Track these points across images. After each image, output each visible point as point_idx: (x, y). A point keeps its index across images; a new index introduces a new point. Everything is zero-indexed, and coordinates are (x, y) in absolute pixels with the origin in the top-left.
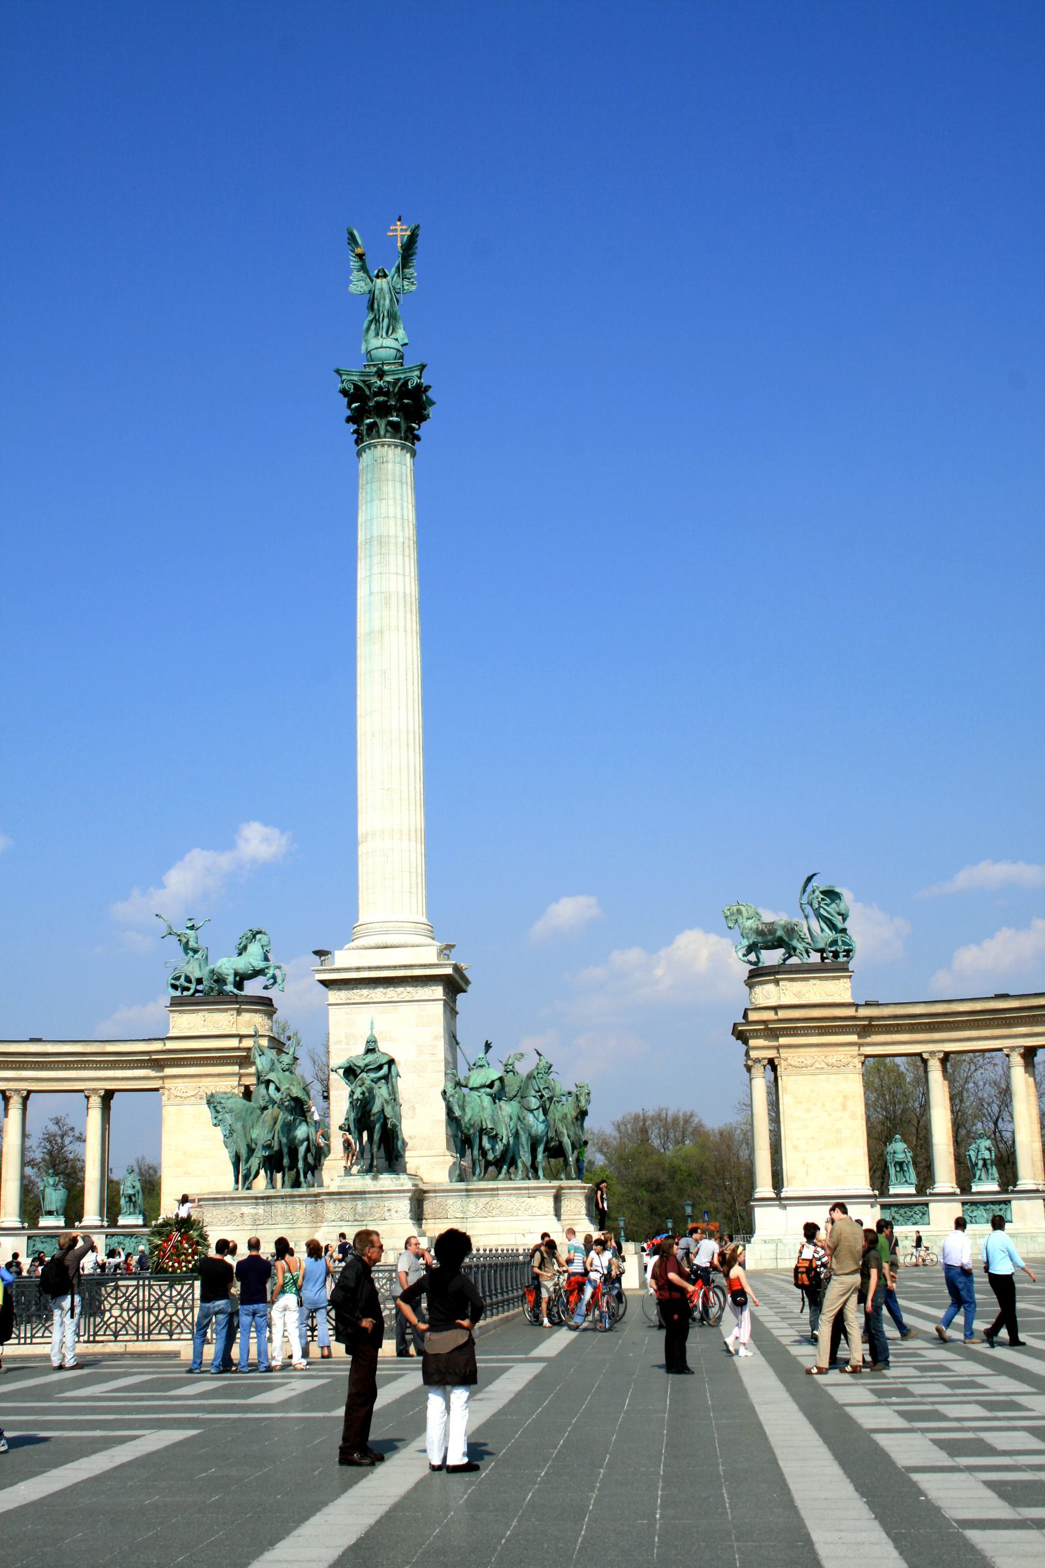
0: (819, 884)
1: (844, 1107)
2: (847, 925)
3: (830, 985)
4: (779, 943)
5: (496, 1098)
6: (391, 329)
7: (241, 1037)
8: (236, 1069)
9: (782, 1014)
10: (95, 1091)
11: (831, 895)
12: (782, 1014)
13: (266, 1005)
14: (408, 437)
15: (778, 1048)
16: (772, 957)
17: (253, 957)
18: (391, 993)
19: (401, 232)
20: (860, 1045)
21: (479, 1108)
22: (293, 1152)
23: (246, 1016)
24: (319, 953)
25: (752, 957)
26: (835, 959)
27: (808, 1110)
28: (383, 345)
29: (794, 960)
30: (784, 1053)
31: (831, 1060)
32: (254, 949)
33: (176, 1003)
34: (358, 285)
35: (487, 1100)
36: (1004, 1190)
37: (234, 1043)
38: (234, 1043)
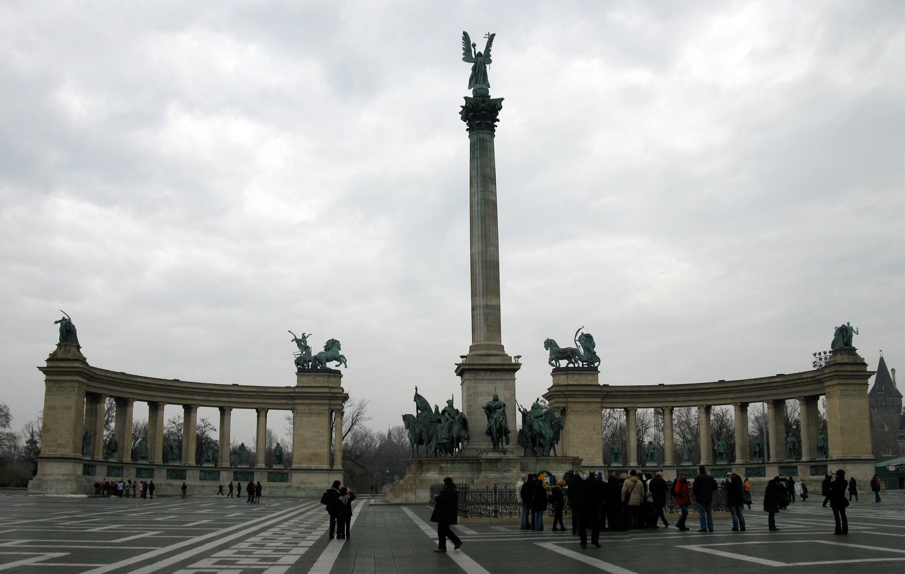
1: (594, 429)
2: (595, 349)
3: (590, 377)
7: (330, 388)
9: (569, 388)
10: (262, 409)
12: (569, 388)
15: (567, 402)
16: (563, 363)
18: (493, 376)
20: (603, 403)
25: (554, 362)
29: (571, 365)
30: (570, 405)
31: (590, 409)
35: (541, 423)
37: (327, 390)
38: (327, 390)
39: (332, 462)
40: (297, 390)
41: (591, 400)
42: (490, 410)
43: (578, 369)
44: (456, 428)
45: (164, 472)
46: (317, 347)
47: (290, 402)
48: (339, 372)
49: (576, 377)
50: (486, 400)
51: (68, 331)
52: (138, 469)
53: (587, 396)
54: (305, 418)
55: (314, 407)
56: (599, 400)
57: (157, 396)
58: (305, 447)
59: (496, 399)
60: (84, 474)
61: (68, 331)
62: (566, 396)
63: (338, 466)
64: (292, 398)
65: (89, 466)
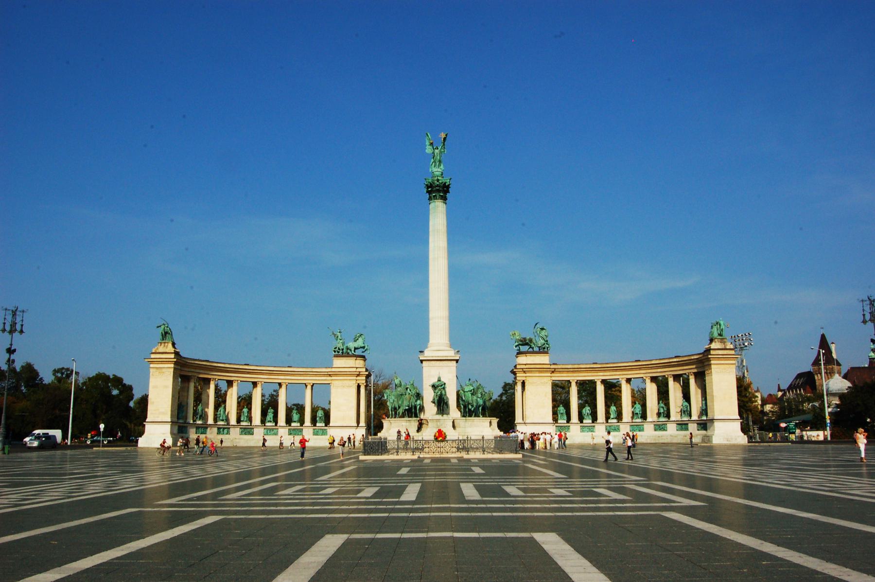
4: (527, 344)
5: (472, 394)
6: (440, 165)
9: (527, 366)
12: (527, 366)
13: (363, 357)
14: (444, 199)
17: (360, 343)
19: (443, 136)
21: (468, 397)
22: (415, 407)
23: (358, 361)
26: (543, 350)
28: (437, 170)
32: (360, 340)
33: (336, 356)
34: (429, 150)
36: (593, 422)
37: (355, 370)
38: (355, 370)
39: (358, 422)
42: (434, 387)
44: (413, 400)
45: (238, 430)
47: (329, 378)
48: (363, 357)
50: (434, 380)
52: (219, 429)
57: (232, 376)
59: (439, 380)
60: (179, 432)
62: (524, 372)
63: (363, 423)
64: (330, 375)
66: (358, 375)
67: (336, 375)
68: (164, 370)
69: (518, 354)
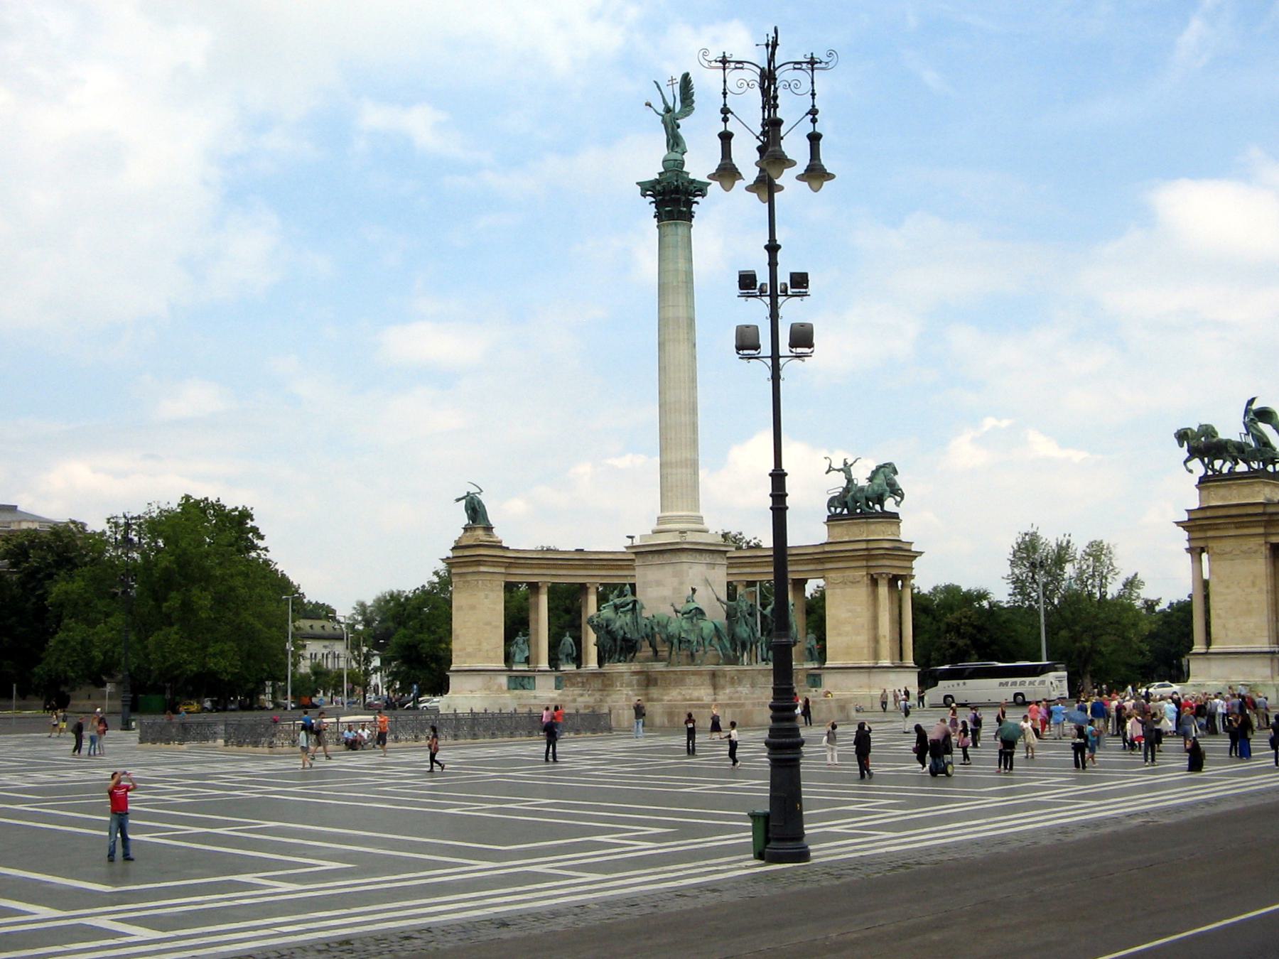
0: (1255, 406)
3: (1246, 490)
8: (864, 563)
11: (1265, 415)
24: (632, 537)
27: (1228, 587)
37: (863, 546)
40: (827, 548)
41: (1246, 531)
43: (1232, 476)
46: (861, 477)
47: (820, 567)
48: (895, 516)
49: (1222, 492)
51: (475, 510)
53: (1239, 526)
54: (838, 591)
55: (848, 573)
56: (1261, 530)
58: (839, 635)
61: (475, 510)
62: (1202, 528)
64: (820, 561)
65: (523, 677)
66: (869, 557)
67: (830, 560)
68: (469, 578)
69: (1204, 482)
